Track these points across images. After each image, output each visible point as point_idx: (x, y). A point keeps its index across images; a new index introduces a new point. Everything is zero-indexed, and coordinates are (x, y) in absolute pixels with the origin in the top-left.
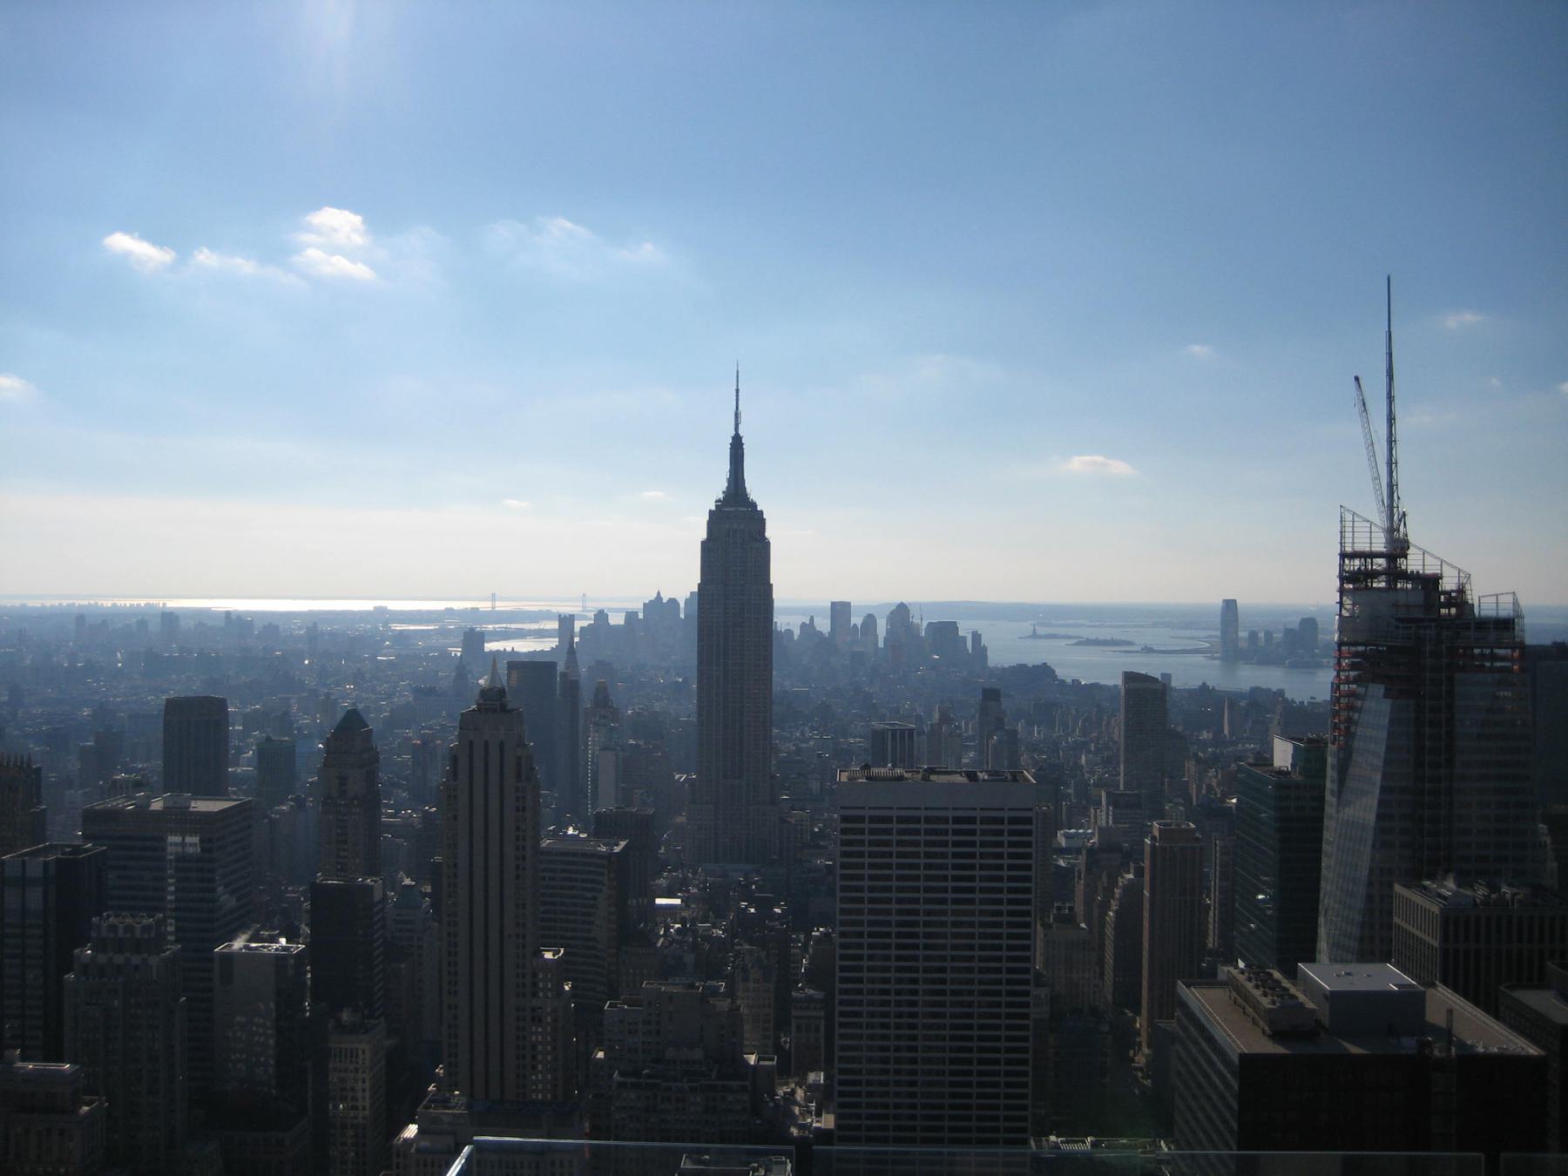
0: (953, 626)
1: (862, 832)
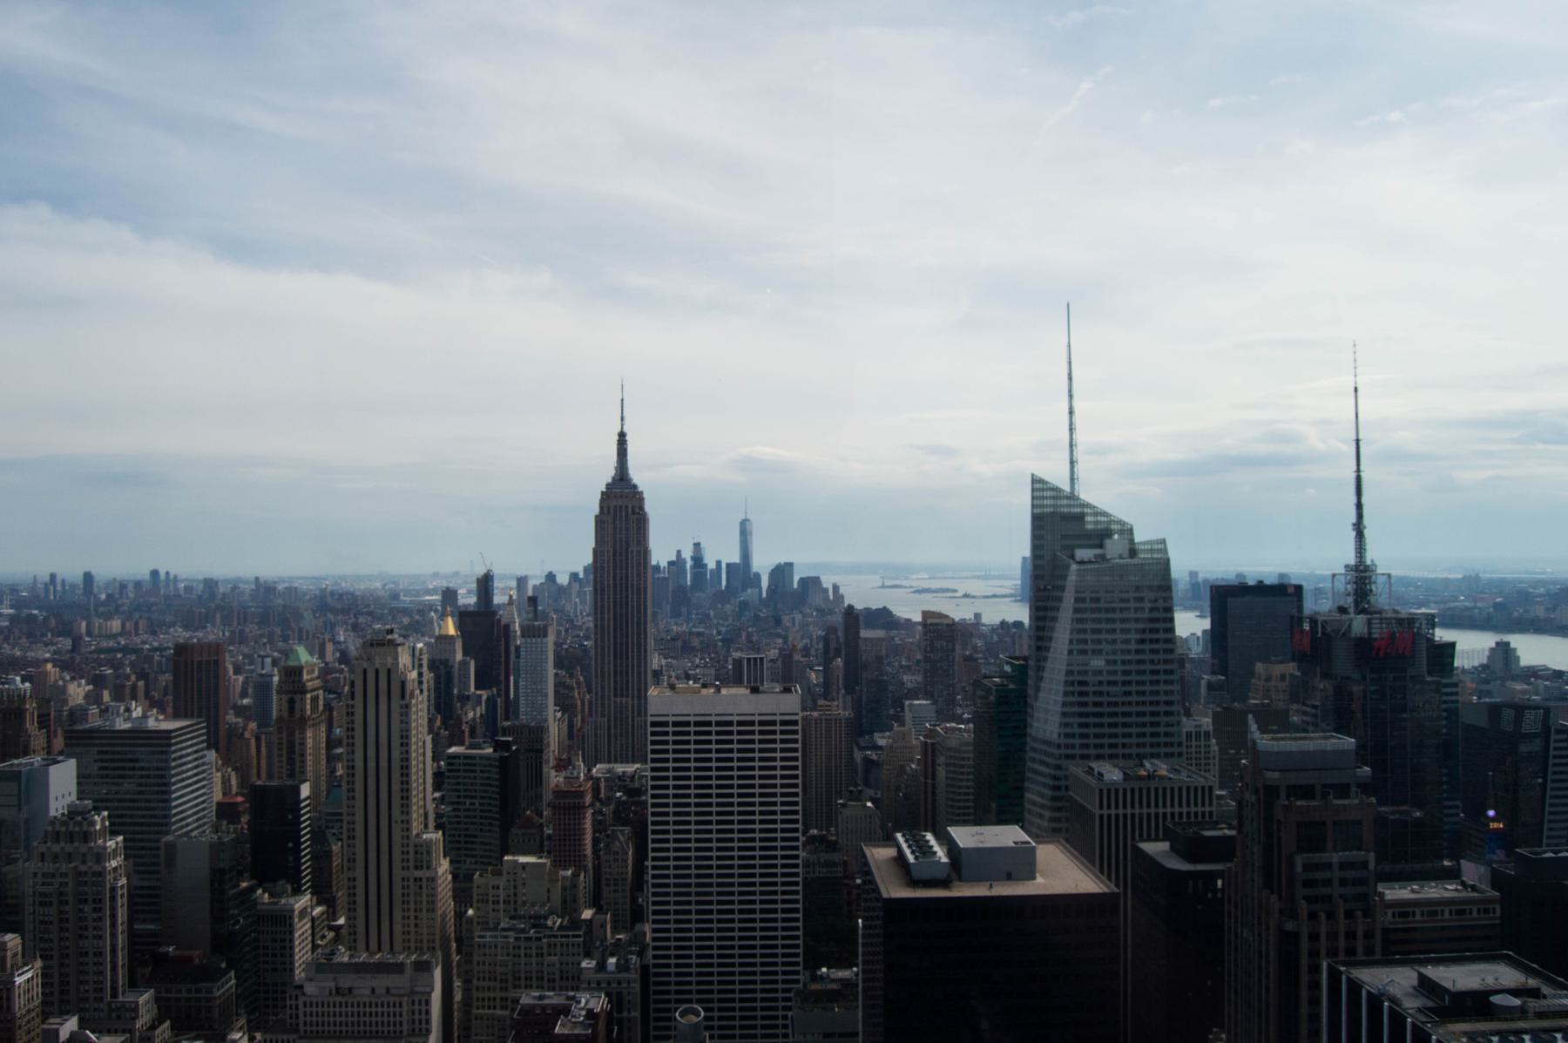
0: (816, 581)
1: (688, 733)
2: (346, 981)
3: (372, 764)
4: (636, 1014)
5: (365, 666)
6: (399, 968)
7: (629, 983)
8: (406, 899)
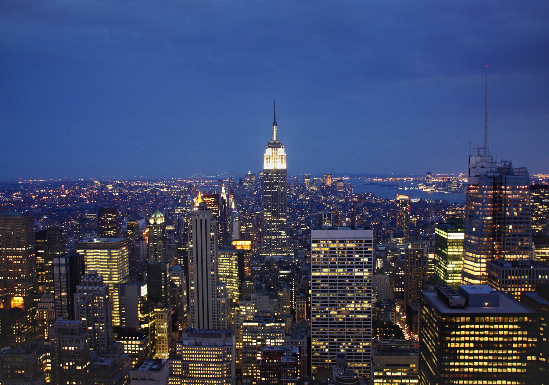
2: (199, 340)
3: (199, 257)
4: (306, 355)
5: (196, 218)
6: (219, 336)
7: (304, 343)
8: (214, 309)
